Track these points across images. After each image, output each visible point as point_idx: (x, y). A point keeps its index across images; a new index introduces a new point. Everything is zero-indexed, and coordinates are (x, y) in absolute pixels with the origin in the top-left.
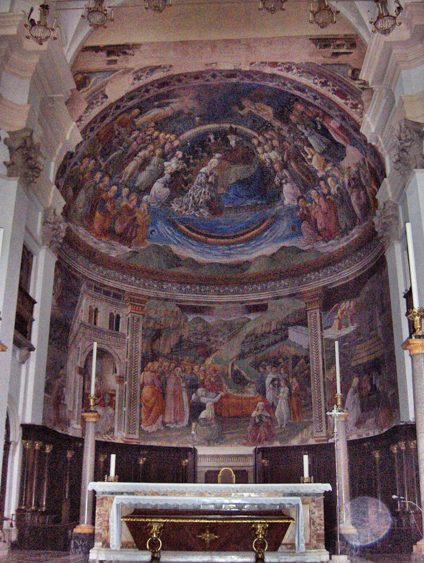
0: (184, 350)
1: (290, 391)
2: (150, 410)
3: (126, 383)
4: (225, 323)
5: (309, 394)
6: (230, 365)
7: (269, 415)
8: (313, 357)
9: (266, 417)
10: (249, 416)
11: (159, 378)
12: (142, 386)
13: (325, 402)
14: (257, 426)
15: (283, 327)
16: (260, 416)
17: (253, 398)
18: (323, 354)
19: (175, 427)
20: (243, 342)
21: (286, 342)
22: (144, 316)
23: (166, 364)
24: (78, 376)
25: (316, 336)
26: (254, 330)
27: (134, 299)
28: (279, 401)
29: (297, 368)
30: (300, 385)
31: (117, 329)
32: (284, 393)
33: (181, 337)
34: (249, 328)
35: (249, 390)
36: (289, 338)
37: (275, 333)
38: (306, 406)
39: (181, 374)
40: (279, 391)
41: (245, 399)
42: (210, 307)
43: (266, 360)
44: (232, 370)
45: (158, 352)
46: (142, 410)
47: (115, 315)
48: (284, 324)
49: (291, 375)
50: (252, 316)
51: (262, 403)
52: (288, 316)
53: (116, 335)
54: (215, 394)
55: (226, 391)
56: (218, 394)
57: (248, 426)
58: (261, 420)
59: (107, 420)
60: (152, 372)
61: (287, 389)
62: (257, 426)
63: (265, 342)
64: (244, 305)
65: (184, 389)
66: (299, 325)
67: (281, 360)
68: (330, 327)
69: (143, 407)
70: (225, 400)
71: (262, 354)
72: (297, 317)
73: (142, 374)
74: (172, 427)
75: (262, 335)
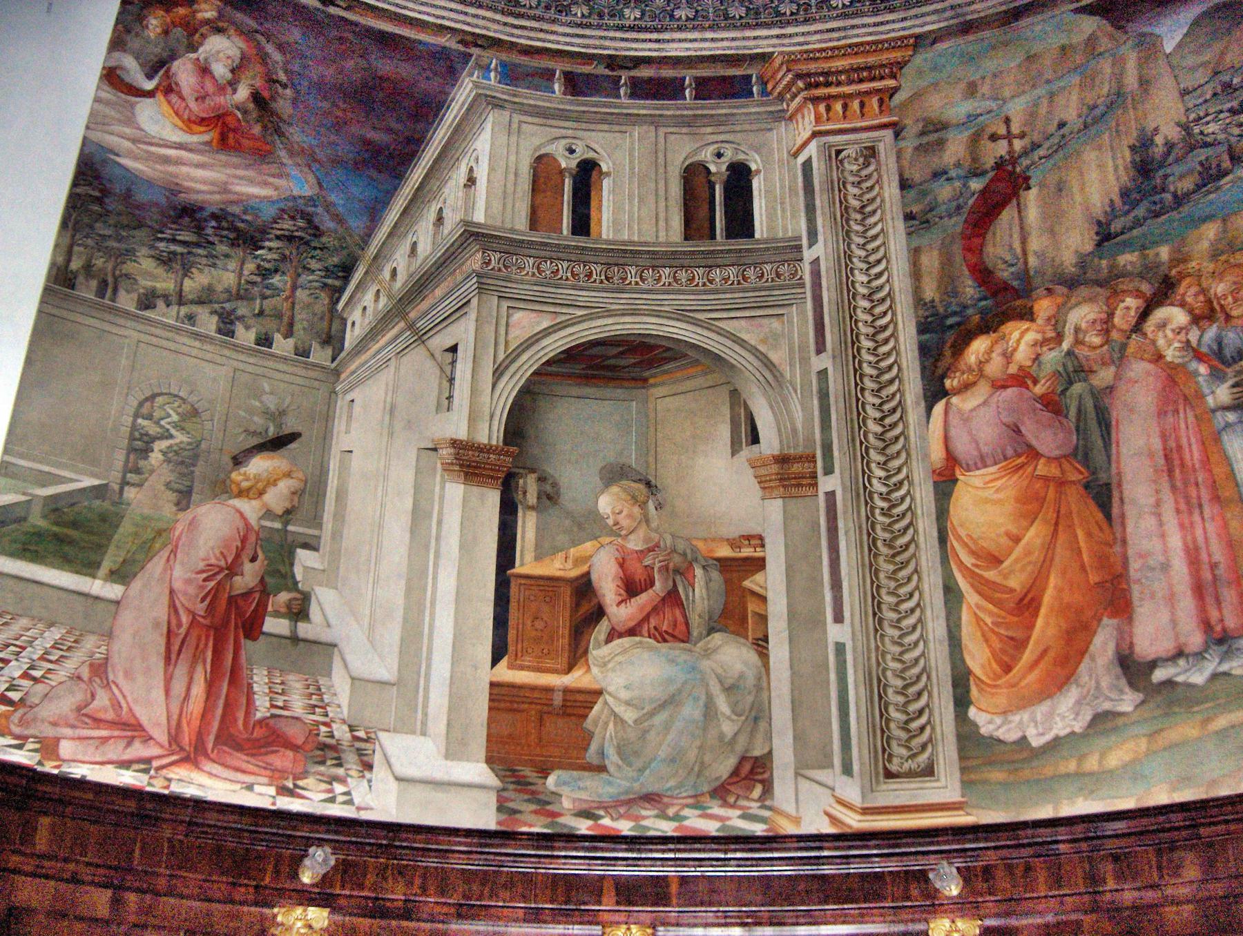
0: (1179, 200)
2: (1027, 605)
3: (827, 484)
11: (1052, 405)
12: (945, 482)
19: (1215, 676)
22: (897, 130)
23: (1082, 315)
24: (456, 491)
27: (826, 74)
31: (741, 223)
33: (1144, 143)
39: (1194, 336)
45: (1025, 275)
46: (965, 616)
47: (718, 168)
53: (741, 260)
59: (710, 711)
60: (999, 385)
65: (1231, 417)
69: (971, 597)
73: (939, 408)
74: (1198, 678)
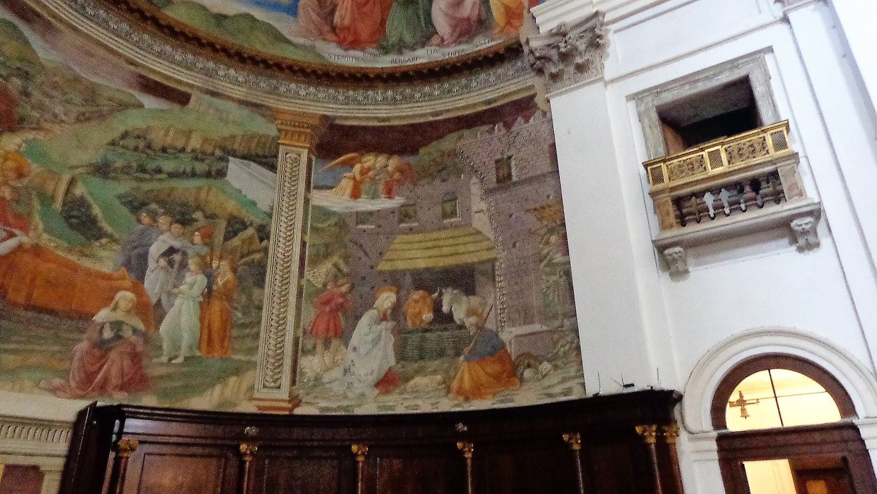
1: (209, 287)
4: (77, 79)
5: (256, 303)
6: (66, 177)
7: (141, 327)
8: (279, 229)
9: (135, 331)
10: (86, 317)
13: (297, 326)
14: (102, 347)
15: (218, 153)
16: (117, 325)
17: (108, 277)
18: (304, 231)
20: (113, 143)
21: (218, 183)
25: (293, 194)
26: (148, 129)
28: (178, 302)
29: (236, 242)
30: (240, 279)
32: (192, 286)
34: (133, 121)
35: (103, 253)
36: (228, 178)
37: (198, 156)
38: (244, 326)
40: (180, 278)
41: (88, 273)
42: (49, 23)
43: (162, 203)
44: (68, 191)
48: (223, 149)
49: (217, 252)
50: (150, 102)
51: (130, 295)
52: (234, 137)
54: (4, 234)
55: (39, 237)
56: (11, 235)
57: (80, 340)
58: (118, 337)
61: (201, 280)
62: (102, 347)
63: (168, 166)
64: (133, 68)
66: (254, 161)
67: (198, 215)
68: (331, 188)
70: (27, 258)
71: (154, 185)
72: (253, 146)
75: (164, 150)
